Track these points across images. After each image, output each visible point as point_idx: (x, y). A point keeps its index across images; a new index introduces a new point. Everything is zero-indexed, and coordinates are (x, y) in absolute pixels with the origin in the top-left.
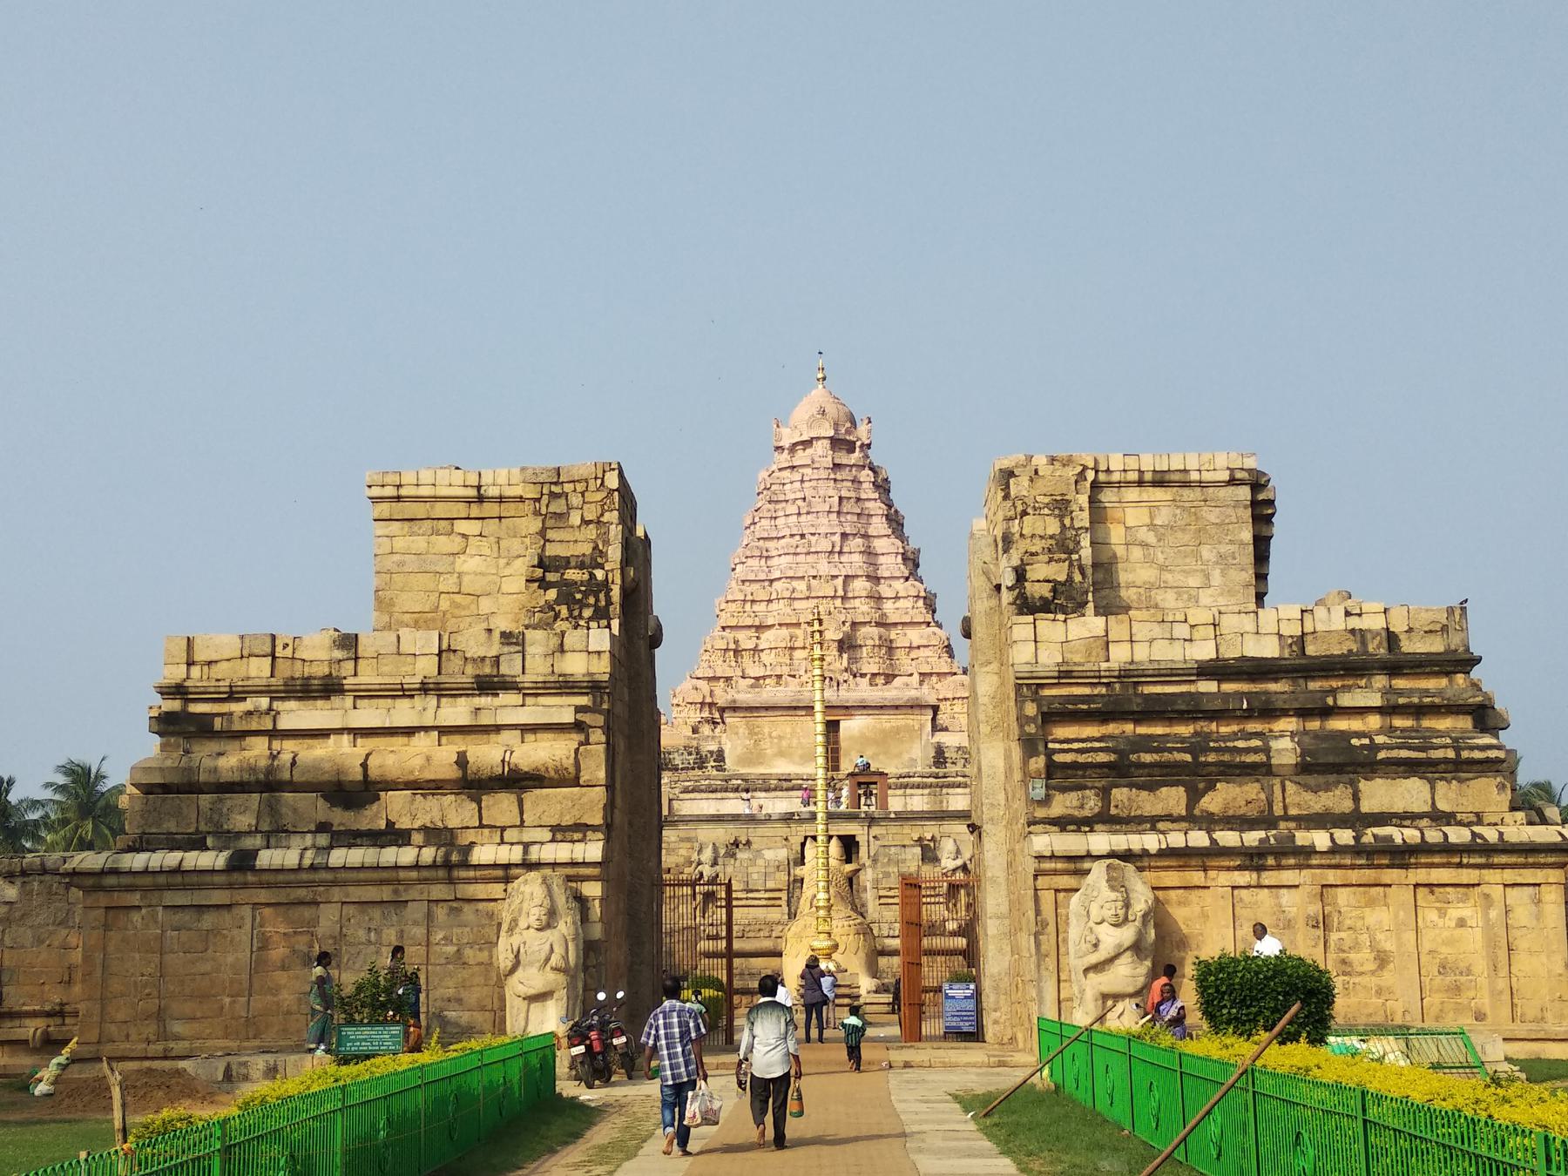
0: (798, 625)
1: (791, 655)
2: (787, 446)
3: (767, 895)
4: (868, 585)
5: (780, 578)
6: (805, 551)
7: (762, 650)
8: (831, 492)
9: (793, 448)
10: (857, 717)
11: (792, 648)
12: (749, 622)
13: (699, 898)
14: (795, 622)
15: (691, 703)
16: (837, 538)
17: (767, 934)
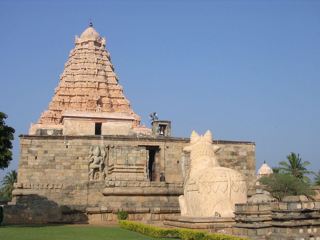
0: (83, 96)
1: (81, 105)
2: (81, 43)
3: (137, 167)
4: (106, 85)
5: (78, 81)
6: (86, 73)
7: (71, 103)
8: (94, 57)
9: (82, 44)
10: (108, 122)
11: (81, 103)
12: (68, 94)
13: (92, 170)
14: (82, 95)
15: (49, 117)
16: (96, 71)
17: (138, 185)
